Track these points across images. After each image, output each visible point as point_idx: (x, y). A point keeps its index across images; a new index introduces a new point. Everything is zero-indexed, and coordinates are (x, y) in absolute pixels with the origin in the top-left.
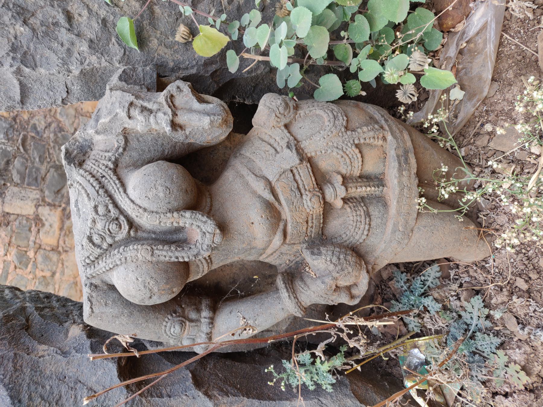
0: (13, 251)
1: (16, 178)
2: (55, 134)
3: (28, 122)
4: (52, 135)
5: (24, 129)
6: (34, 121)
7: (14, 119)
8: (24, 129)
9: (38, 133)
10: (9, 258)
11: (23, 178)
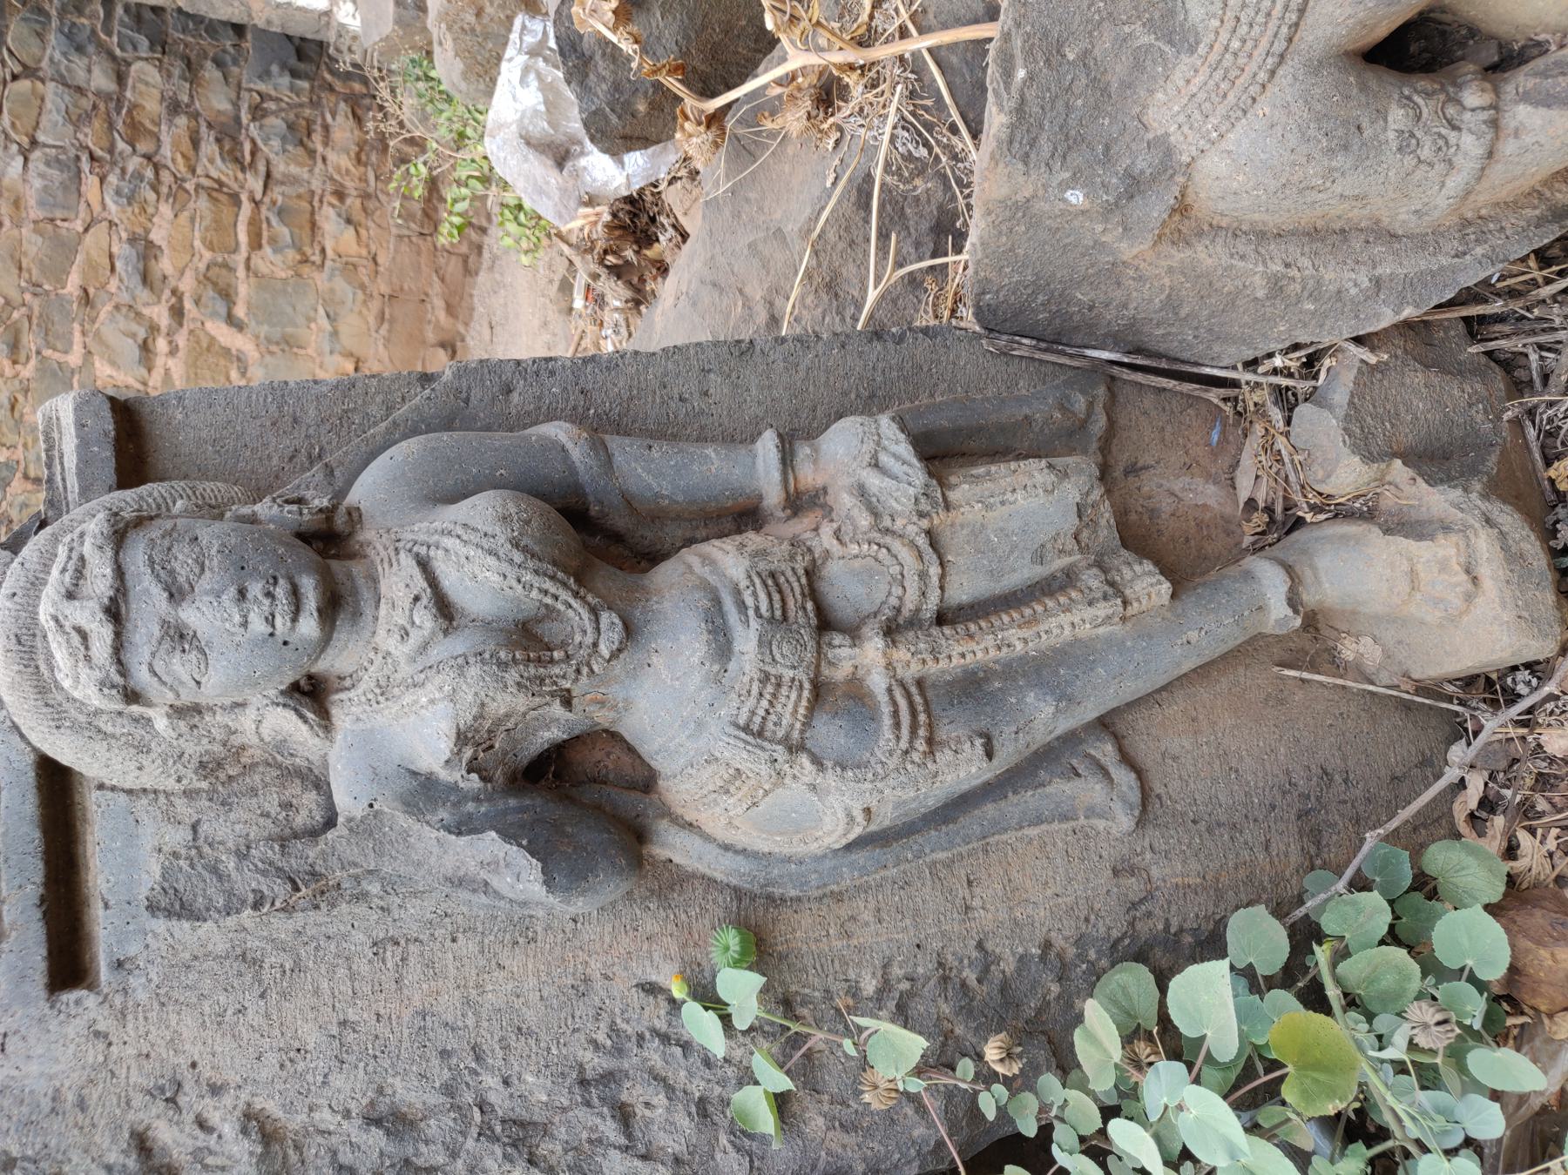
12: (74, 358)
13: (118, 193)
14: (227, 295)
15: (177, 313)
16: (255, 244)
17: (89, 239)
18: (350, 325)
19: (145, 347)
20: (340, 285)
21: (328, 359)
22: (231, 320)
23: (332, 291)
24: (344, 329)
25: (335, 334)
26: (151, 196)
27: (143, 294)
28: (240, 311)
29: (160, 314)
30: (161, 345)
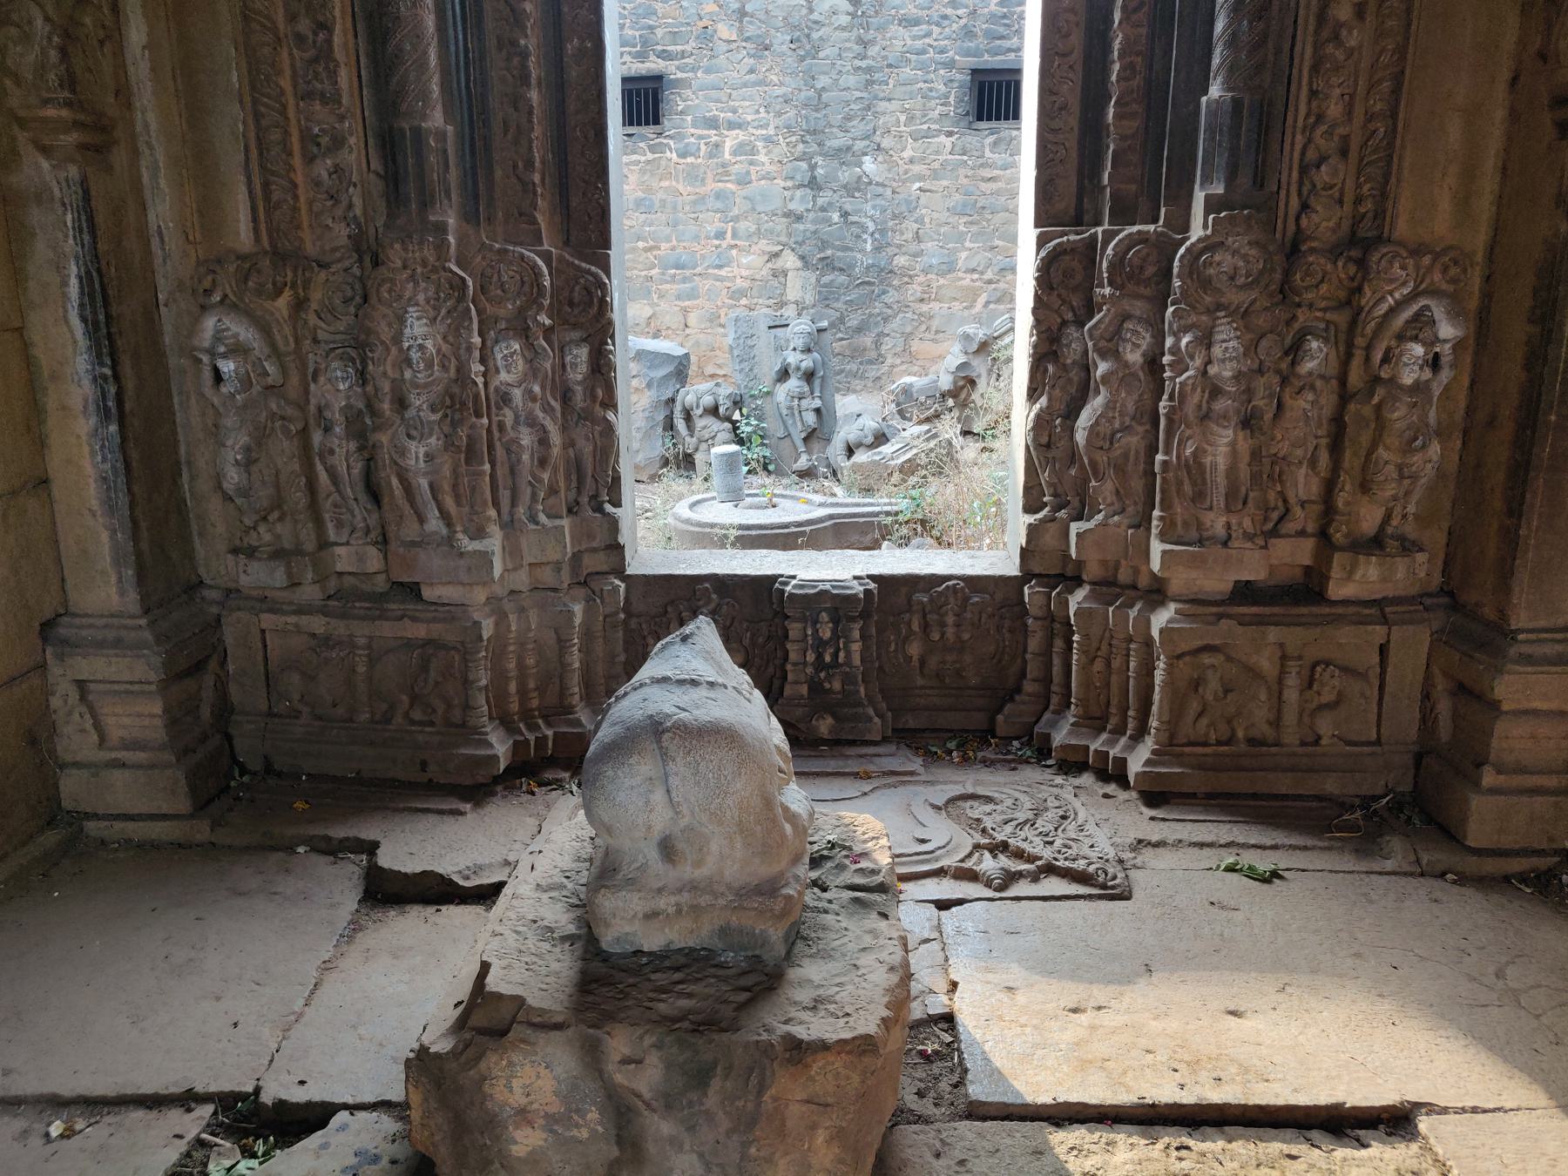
0: (746, 284)
1: (826, 279)
2: (879, 315)
3: (889, 285)
4: (877, 311)
5: (881, 282)
6: (892, 292)
7: (891, 271)
8: (881, 282)
9: (879, 296)
10: (739, 281)
11: (825, 286)
12: (968, 244)
14: (998, 301)
15: (990, 282)
19: (974, 270)
22: (988, 303)
27: (996, 269)
28: (992, 306)
29: (989, 275)
30: (976, 276)
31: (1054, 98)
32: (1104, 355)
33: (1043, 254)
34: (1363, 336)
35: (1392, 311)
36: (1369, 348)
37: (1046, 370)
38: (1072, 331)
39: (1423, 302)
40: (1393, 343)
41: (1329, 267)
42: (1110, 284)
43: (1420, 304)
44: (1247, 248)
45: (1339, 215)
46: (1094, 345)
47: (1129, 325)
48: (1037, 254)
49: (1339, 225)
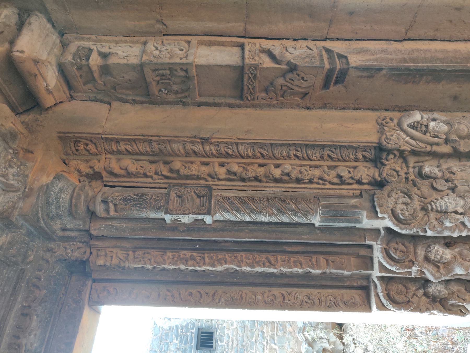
13: (260, 325)
14: (274, 339)
15: (267, 343)
16: (277, 331)
17: (256, 332)
18: (292, 343)
19: (263, 349)
20: (290, 336)
21: (289, 349)
22: (275, 344)
23: (289, 337)
24: (291, 344)
25: (289, 345)
26: (264, 324)
27: (263, 340)
28: (276, 342)
29: (265, 343)
30: (265, 348)
31: (304, 302)
32: (450, 271)
33: (390, 306)
34: (426, 147)
35: (412, 138)
36: (432, 144)
37: (452, 305)
38: (432, 289)
39: (405, 126)
40: (429, 135)
41: (388, 167)
42: (410, 267)
43: (407, 127)
44: (392, 198)
45: (362, 167)
46: (444, 276)
47: (432, 257)
48: (390, 310)
49: (366, 167)
